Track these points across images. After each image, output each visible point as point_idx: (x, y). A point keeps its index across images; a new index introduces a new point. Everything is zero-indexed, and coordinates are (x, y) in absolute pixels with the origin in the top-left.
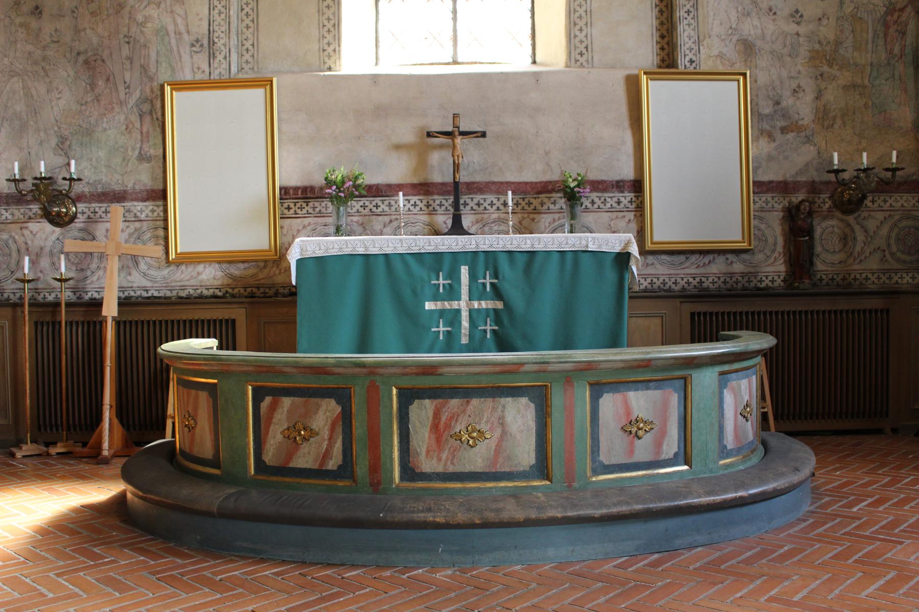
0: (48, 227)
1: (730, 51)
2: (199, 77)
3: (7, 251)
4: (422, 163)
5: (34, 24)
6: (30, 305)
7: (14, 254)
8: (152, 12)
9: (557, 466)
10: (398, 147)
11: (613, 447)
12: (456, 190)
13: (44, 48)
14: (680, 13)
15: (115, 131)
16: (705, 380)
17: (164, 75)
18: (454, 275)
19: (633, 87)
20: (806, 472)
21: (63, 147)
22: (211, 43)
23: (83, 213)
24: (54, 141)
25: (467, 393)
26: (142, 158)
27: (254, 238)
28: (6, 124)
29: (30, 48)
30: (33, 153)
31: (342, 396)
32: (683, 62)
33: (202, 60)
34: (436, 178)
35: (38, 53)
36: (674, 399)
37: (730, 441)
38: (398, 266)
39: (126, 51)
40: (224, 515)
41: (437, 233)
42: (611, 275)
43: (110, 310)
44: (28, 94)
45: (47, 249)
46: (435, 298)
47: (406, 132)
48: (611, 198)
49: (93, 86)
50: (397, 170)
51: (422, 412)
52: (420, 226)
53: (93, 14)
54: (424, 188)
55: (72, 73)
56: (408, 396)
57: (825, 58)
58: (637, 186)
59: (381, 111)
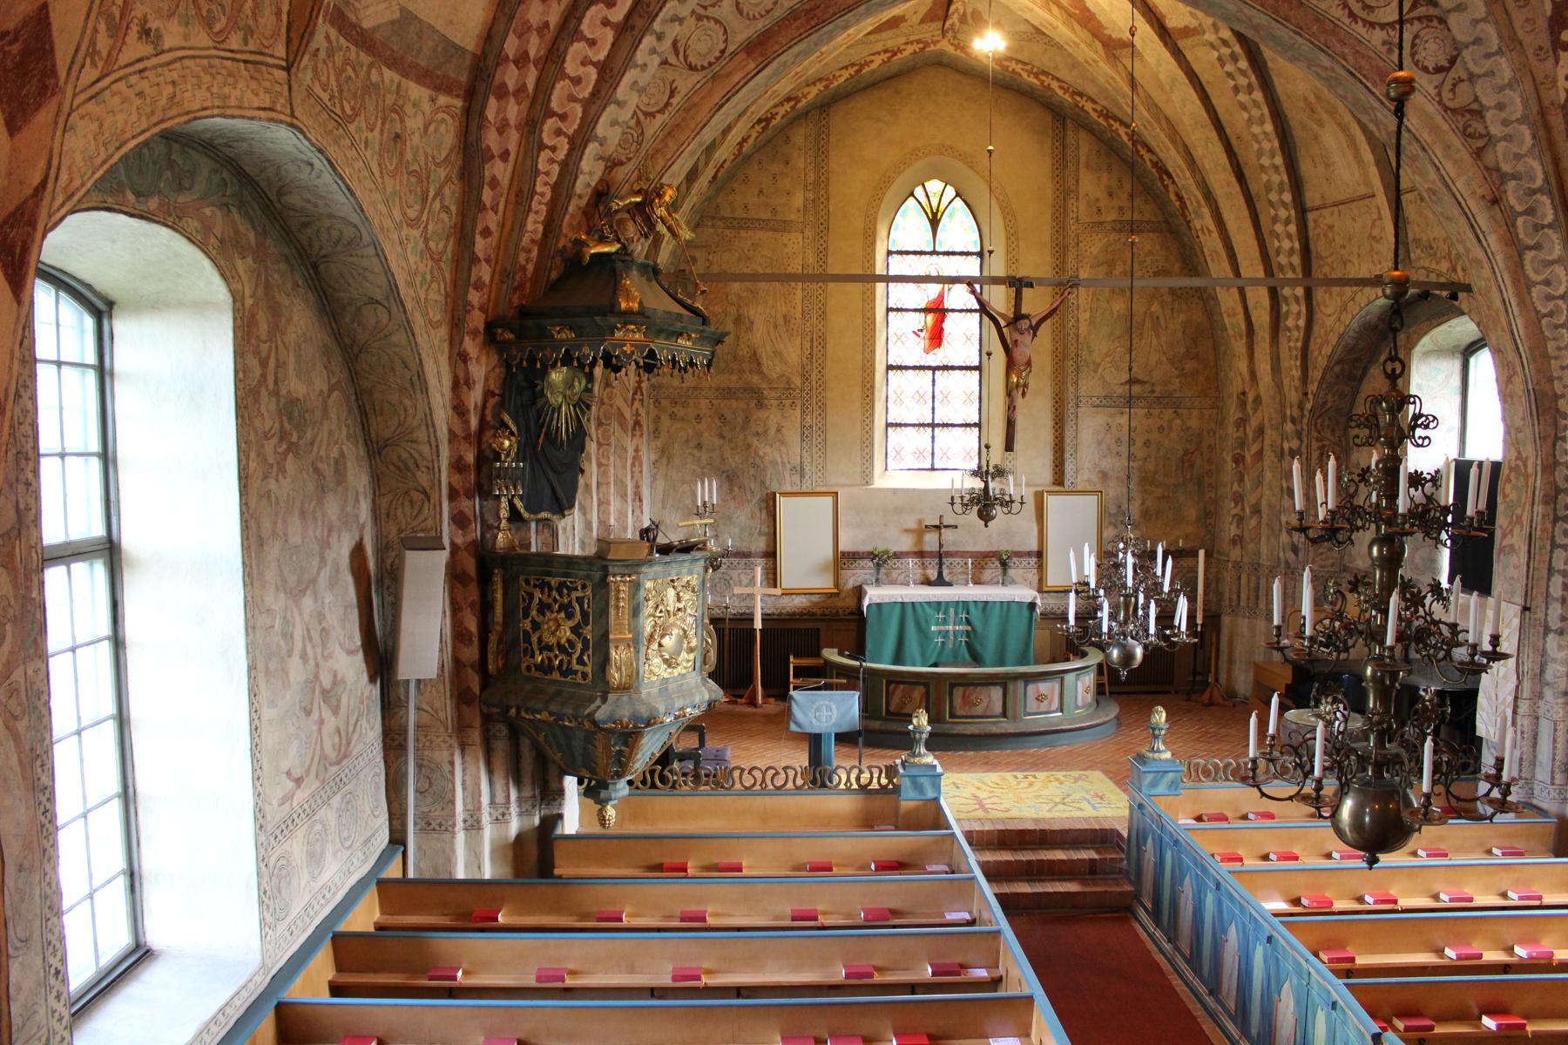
1: (1094, 478)
2: (795, 489)
4: (920, 540)
8: (768, 450)
9: (1010, 713)
10: (907, 531)
11: (1032, 705)
12: (940, 556)
14: (1067, 455)
15: (745, 517)
16: (1069, 677)
17: (774, 487)
18: (946, 612)
19: (1039, 500)
20: (1112, 716)
22: (802, 470)
25: (976, 685)
26: (760, 533)
27: (824, 583)
31: (926, 685)
32: (1067, 483)
33: (797, 478)
34: (927, 548)
36: (1057, 686)
37: (1080, 703)
38: (919, 609)
39: (752, 471)
40: (881, 732)
41: (928, 582)
42: (1026, 613)
43: (758, 625)
46: (937, 624)
47: (912, 525)
48: (1025, 561)
49: (731, 491)
50: (906, 544)
51: (958, 692)
52: (918, 577)
54: (921, 554)
56: (952, 686)
57: (1147, 481)
58: (1040, 554)
59: (898, 510)
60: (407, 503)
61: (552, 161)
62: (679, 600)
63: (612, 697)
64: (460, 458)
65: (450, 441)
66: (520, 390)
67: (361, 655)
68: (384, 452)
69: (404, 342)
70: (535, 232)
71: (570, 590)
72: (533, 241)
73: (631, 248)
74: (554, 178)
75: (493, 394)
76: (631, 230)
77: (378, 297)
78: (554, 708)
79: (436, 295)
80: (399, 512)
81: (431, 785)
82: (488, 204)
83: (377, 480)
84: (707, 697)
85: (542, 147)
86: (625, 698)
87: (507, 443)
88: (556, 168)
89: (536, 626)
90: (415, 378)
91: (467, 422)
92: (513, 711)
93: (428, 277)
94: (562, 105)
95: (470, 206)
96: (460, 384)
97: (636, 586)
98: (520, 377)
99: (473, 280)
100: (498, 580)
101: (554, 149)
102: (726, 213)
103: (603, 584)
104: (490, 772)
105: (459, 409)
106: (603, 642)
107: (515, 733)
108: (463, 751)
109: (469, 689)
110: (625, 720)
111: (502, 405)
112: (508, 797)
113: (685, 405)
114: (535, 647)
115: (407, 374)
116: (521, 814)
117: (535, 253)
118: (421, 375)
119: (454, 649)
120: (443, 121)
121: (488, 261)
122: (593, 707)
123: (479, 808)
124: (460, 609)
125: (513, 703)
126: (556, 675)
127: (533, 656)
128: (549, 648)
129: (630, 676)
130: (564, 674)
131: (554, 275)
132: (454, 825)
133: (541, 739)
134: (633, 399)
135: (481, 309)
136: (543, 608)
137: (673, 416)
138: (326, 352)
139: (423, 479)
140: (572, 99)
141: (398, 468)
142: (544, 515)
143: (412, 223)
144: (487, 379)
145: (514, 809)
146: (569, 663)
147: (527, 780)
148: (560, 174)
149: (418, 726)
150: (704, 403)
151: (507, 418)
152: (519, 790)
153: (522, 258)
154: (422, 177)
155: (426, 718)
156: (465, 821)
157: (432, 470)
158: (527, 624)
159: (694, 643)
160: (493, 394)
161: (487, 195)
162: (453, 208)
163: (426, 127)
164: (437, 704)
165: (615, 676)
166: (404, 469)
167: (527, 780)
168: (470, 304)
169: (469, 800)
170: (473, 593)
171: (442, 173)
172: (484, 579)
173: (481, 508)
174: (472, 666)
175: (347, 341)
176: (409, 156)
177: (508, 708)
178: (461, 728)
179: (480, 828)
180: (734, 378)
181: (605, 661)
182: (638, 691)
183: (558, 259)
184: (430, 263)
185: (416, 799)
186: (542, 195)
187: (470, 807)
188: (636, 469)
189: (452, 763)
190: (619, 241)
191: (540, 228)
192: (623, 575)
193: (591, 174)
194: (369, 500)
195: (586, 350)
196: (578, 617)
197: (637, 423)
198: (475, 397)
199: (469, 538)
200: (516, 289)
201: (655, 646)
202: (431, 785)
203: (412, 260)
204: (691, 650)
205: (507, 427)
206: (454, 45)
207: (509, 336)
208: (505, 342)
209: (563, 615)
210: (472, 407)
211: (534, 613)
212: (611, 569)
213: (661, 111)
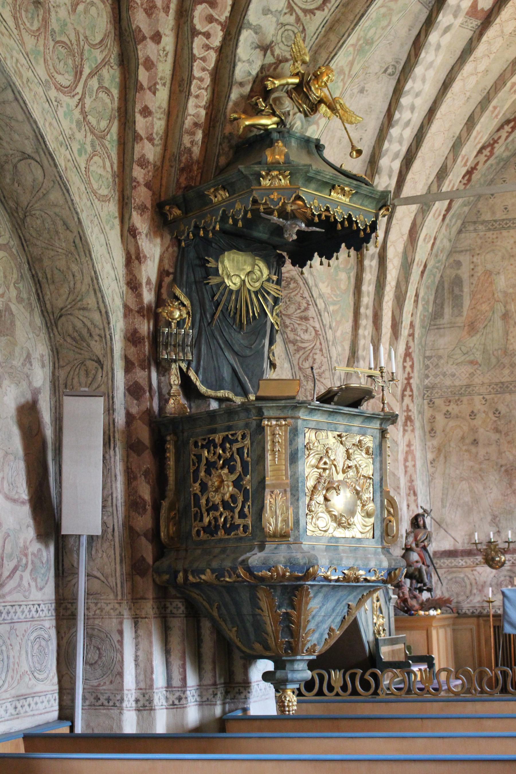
0: (488, 569)
3: (463, 584)
5: (474, 450)
6: (493, 616)
7: (469, 587)
13: (481, 463)
21: (495, 520)
23: (509, 560)
24: (489, 518)
28: (459, 509)
29: (471, 464)
30: (477, 526)
35: (477, 467)
44: (472, 491)
45: (488, 583)
53: (509, 442)
55: (498, 478)
60: (83, 373)
62: (349, 458)
63: (269, 547)
64: (135, 331)
65: (125, 316)
66: (191, 266)
67: (26, 509)
68: (60, 323)
69: (61, 201)
70: (197, 115)
71: (231, 442)
72: (196, 124)
73: (289, 121)
74: (211, 64)
75: (168, 274)
76: (288, 105)
77: (29, 150)
78: (215, 564)
79: (102, 170)
80: (76, 380)
81: (100, 657)
82: (145, 84)
83: (56, 352)
84: (385, 564)
85: (195, 33)
86: (283, 547)
87: (177, 314)
88: (212, 56)
89: (204, 487)
90: (77, 240)
91: (139, 296)
92: (181, 576)
93: (89, 149)
95: (129, 87)
96: (133, 259)
97: (294, 432)
98: (192, 254)
99: (136, 157)
100: (170, 446)
101: (207, 35)
102: (487, 217)
103: (261, 429)
104: (167, 652)
105: (133, 285)
106: (261, 485)
107: (194, 614)
108: (136, 624)
109: (143, 559)
110: (281, 567)
111: (174, 280)
112: (184, 680)
113: (459, 402)
114: (204, 510)
115: (71, 237)
116: (202, 704)
117: (199, 135)
118: (82, 237)
119: (128, 518)
121: (150, 139)
122: (248, 555)
123: (151, 687)
124: (135, 478)
125: (180, 566)
126: (221, 533)
127: (201, 520)
128: (215, 508)
129: (285, 521)
130: (228, 532)
131: (223, 161)
132: (122, 700)
133: (215, 614)
134: (403, 396)
135: (148, 185)
136: (210, 466)
137: (447, 415)
139: (97, 348)
141: (74, 339)
142: (221, 393)
143: (68, 90)
144: (161, 260)
145: (192, 694)
146: (232, 517)
147: (208, 666)
148: (218, 61)
149: (88, 594)
150: (477, 399)
151: (178, 292)
152: (201, 677)
153: (186, 140)
154: (75, 53)
155: (96, 585)
156: (137, 701)
157: (106, 339)
158: (196, 487)
159: (370, 507)
160: (168, 274)
161: (143, 75)
162: (115, 92)
163: (74, 6)
164: (108, 570)
165: (272, 522)
166: (80, 340)
167: (208, 666)
168: (134, 180)
169: (142, 677)
170: (147, 461)
171: (98, 55)
172: (159, 450)
173: (159, 383)
174: (145, 535)
175: (12, 204)
176: (54, 24)
177: (175, 574)
178: (135, 599)
179: (152, 709)
180: (506, 372)
181: (261, 509)
182: (297, 541)
183: (225, 146)
184: (90, 137)
185: (85, 670)
186: (201, 80)
187: (142, 685)
188: (410, 464)
189: (121, 632)
190: (274, 114)
191: (203, 112)
192: (278, 419)
193: (250, 62)
194: (48, 370)
195: (238, 206)
196: (239, 468)
197: (408, 419)
198: (149, 271)
199: (143, 408)
200: (182, 170)
201: (321, 499)
202: (100, 657)
203: (66, 124)
204: (368, 515)
205: (177, 298)
207: (177, 212)
208: (176, 220)
209: (226, 471)
210: (144, 281)
211: (202, 474)
212: (266, 413)
213: (320, 8)
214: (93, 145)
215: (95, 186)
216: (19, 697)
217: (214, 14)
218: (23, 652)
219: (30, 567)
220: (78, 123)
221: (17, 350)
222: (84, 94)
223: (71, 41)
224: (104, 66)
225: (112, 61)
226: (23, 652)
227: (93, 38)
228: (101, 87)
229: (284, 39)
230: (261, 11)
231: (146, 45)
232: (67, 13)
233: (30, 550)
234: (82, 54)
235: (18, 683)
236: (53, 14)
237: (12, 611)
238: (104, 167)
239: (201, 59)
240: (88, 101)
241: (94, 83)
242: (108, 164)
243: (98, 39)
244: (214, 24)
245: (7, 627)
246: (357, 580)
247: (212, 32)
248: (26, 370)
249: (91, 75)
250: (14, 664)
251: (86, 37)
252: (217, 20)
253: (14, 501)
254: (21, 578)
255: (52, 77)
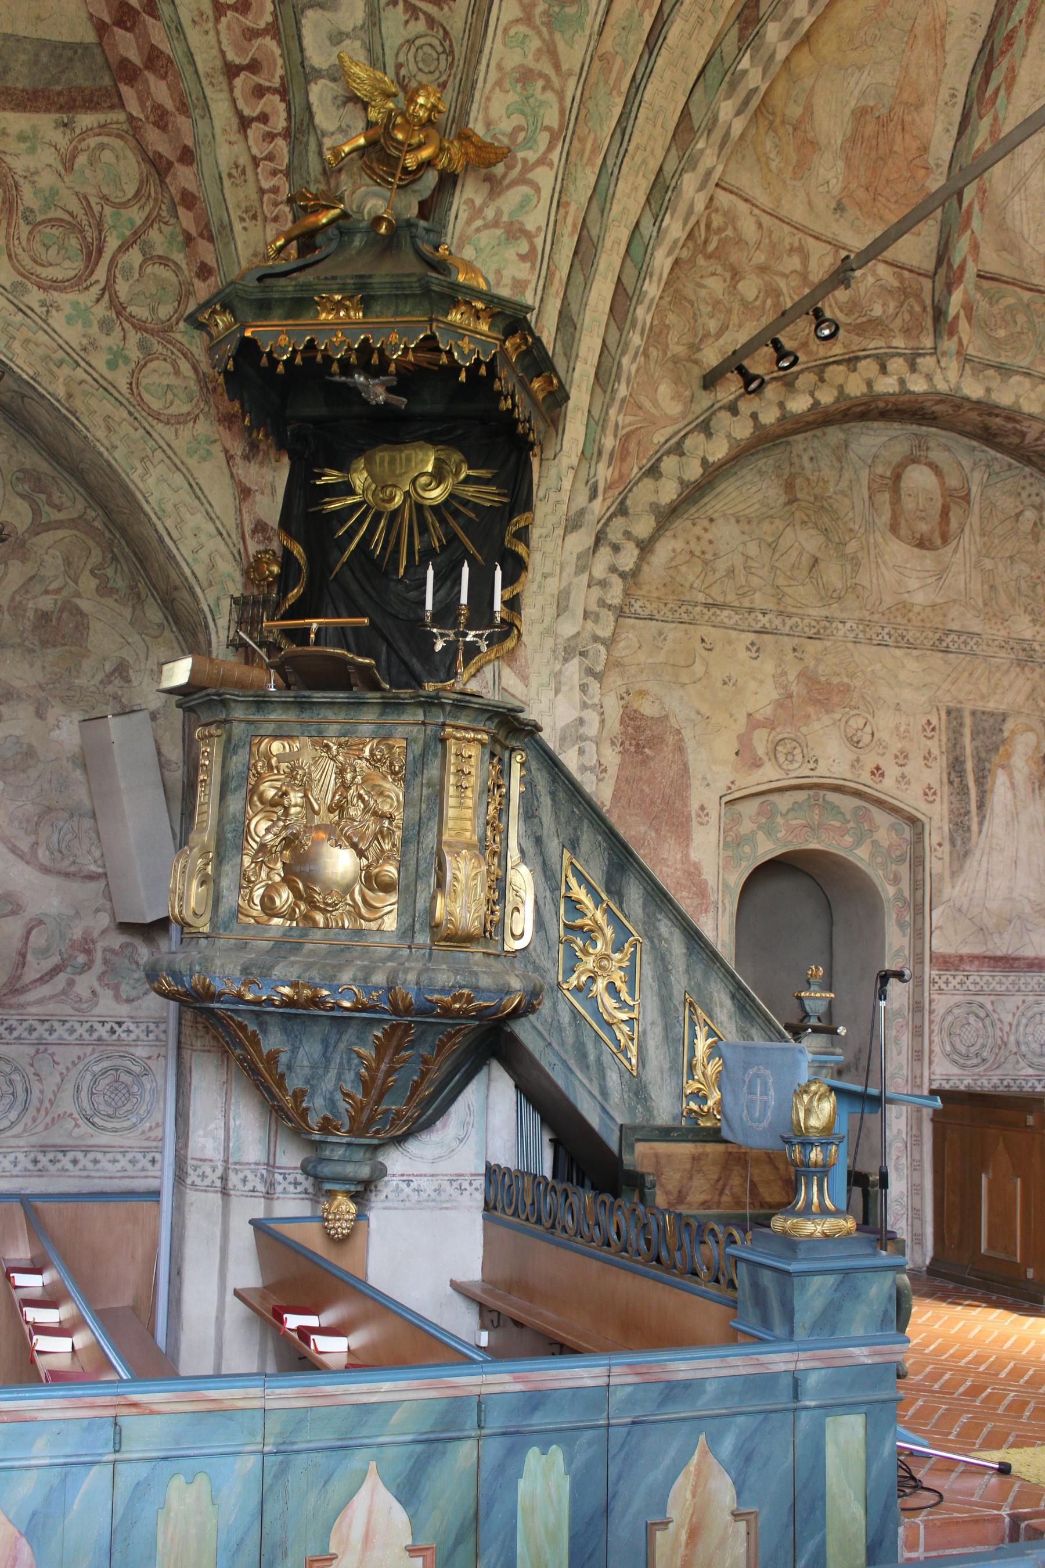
61: (270, 137)
79: (176, 378)
93: (134, 354)
94: (241, 50)
120: (102, 147)
138: (26, 475)
140: (251, 34)
143: (78, 283)
148: (292, 153)
163: (68, 163)
184: (134, 337)
206: (65, 45)
214: (142, 346)
215: (156, 405)
216: (44, 1149)
217: (262, 82)
218: (69, 1087)
219: (98, 967)
220: (106, 326)
221: (87, 665)
222: (111, 280)
223: (71, 214)
224: (152, 225)
225: (164, 214)
226: (69, 1087)
227: (120, 194)
228: (148, 258)
229: (421, 65)
230: (328, 43)
231: (175, 175)
232: (56, 176)
233: (100, 945)
234: (99, 226)
235: (46, 1128)
236: (26, 189)
237: (41, 1029)
238: (177, 372)
239: (266, 158)
240: (123, 288)
241: (135, 256)
242: (185, 366)
243: (131, 191)
244: (268, 97)
245: (31, 1050)
246: (316, 1001)
247: (268, 110)
248: (110, 689)
249: (124, 247)
250: (41, 1102)
251: (105, 198)
252: (269, 89)
253: (67, 875)
254: (71, 983)
255: (27, 275)
